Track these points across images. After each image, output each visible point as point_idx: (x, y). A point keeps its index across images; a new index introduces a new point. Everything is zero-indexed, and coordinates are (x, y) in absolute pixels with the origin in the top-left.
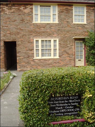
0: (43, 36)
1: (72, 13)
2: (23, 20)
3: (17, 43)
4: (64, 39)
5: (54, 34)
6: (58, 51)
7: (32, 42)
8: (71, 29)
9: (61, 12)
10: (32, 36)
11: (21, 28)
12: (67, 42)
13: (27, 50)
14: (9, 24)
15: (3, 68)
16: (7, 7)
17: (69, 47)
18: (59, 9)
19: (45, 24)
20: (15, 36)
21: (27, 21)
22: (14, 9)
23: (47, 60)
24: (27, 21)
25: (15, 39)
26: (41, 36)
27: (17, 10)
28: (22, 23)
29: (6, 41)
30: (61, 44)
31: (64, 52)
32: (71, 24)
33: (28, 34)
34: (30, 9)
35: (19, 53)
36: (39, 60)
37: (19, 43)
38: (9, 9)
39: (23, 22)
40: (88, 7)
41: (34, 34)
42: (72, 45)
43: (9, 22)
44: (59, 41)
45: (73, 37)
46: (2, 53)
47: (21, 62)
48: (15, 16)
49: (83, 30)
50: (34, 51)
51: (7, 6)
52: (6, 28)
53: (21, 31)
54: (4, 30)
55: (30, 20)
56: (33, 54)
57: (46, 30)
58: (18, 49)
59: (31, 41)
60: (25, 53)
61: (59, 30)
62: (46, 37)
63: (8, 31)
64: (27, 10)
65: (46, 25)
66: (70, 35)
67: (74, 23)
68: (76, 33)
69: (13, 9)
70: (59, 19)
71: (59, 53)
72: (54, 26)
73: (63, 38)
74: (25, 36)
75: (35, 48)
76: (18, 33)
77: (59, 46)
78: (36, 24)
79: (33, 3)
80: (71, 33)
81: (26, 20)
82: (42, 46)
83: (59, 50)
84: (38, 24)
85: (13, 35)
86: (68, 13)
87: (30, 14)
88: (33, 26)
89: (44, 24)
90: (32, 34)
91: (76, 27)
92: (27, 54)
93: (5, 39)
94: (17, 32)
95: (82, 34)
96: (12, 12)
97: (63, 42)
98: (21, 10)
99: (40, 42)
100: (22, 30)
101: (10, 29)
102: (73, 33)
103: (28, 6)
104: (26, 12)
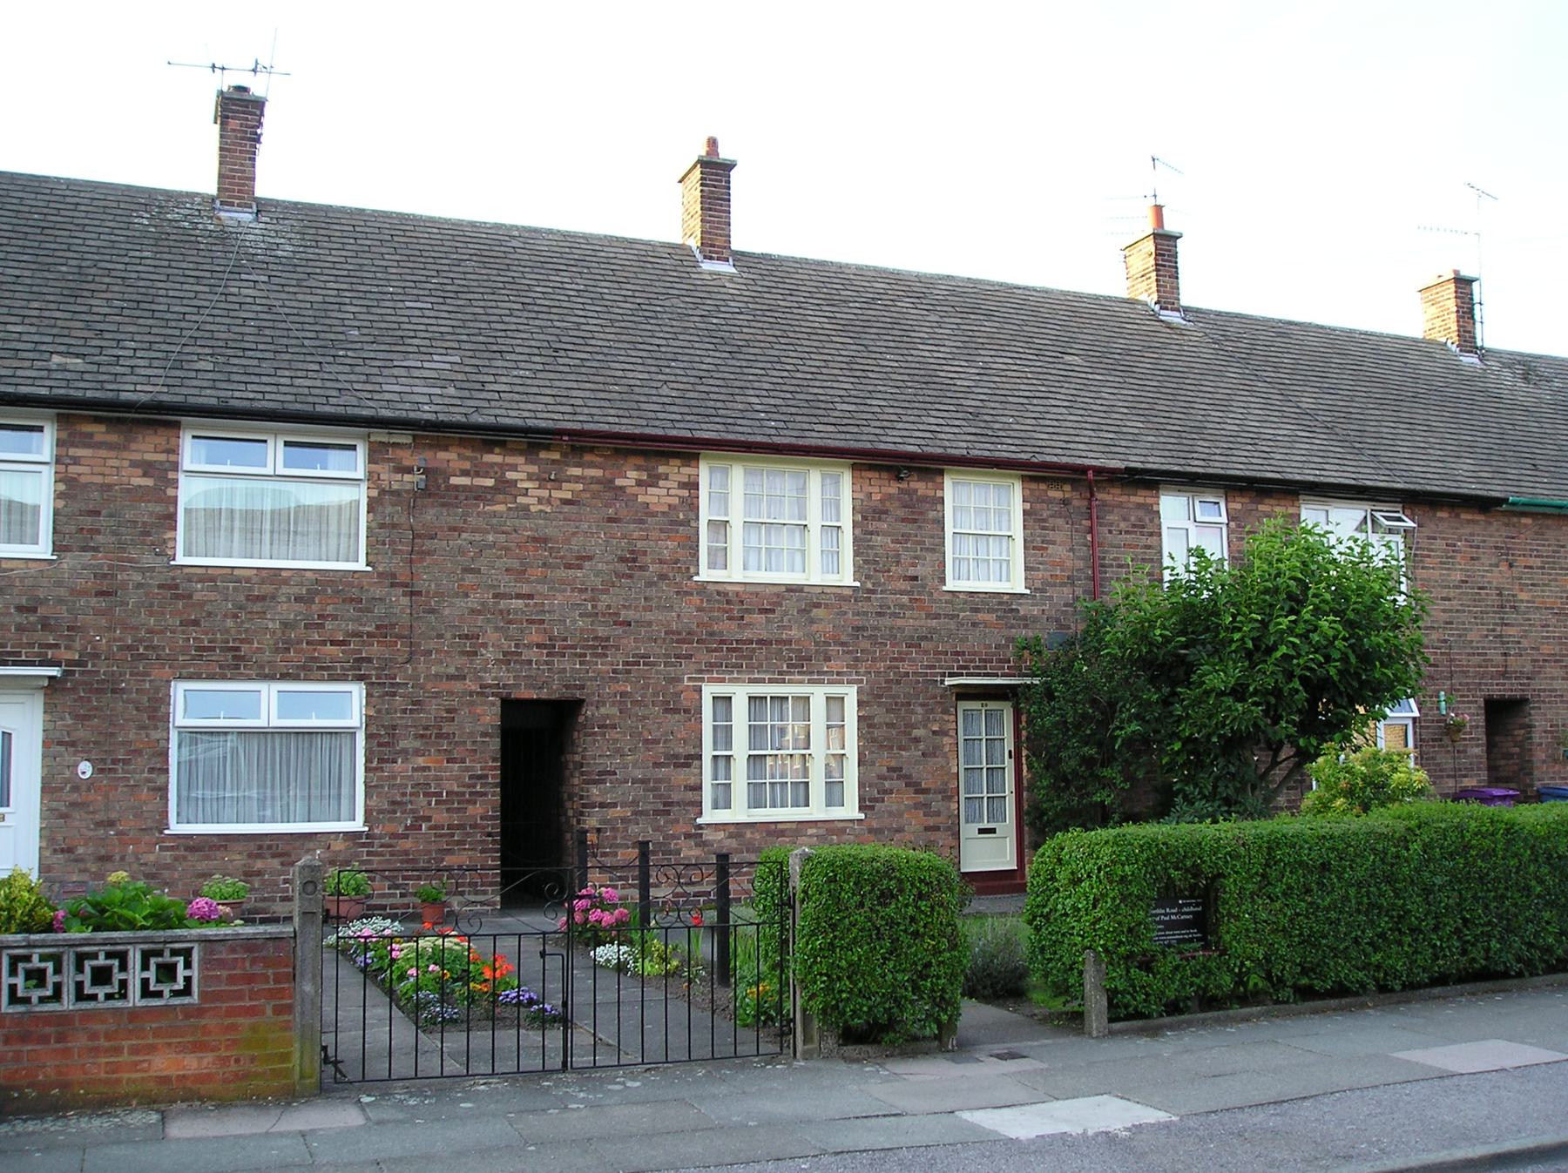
1: (941, 523)
2: (635, 560)
7: (686, 711)
10: (693, 667)
12: (913, 712)
13: (657, 765)
14: (543, 580)
15: (491, 884)
16: (534, 469)
17: (922, 747)
18: (861, 496)
22: (577, 479)
23: (782, 833)
28: (630, 576)
33: (668, 656)
34: (682, 485)
35: (603, 782)
36: (732, 829)
37: (602, 710)
38: (543, 481)
39: (638, 573)
40: (1033, 486)
41: (704, 657)
44: (860, 704)
45: (949, 681)
47: (618, 846)
49: (1005, 632)
53: (620, 630)
54: (510, 622)
56: (699, 788)
60: (643, 781)
61: (857, 629)
62: (780, 673)
63: (534, 627)
65: (778, 595)
67: (951, 585)
71: (861, 785)
72: (827, 606)
73: (887, 682)
75: (708, 752)
76: (602, 646)
78: (720, 588)
80: (937, 653)
82: (755, 732)
86: (915, 521)
88: (696, 599)
95: (1000, 661)
96: (566, 502)
98: (622, 488)
99: (740, 708)
101: (547, 617)
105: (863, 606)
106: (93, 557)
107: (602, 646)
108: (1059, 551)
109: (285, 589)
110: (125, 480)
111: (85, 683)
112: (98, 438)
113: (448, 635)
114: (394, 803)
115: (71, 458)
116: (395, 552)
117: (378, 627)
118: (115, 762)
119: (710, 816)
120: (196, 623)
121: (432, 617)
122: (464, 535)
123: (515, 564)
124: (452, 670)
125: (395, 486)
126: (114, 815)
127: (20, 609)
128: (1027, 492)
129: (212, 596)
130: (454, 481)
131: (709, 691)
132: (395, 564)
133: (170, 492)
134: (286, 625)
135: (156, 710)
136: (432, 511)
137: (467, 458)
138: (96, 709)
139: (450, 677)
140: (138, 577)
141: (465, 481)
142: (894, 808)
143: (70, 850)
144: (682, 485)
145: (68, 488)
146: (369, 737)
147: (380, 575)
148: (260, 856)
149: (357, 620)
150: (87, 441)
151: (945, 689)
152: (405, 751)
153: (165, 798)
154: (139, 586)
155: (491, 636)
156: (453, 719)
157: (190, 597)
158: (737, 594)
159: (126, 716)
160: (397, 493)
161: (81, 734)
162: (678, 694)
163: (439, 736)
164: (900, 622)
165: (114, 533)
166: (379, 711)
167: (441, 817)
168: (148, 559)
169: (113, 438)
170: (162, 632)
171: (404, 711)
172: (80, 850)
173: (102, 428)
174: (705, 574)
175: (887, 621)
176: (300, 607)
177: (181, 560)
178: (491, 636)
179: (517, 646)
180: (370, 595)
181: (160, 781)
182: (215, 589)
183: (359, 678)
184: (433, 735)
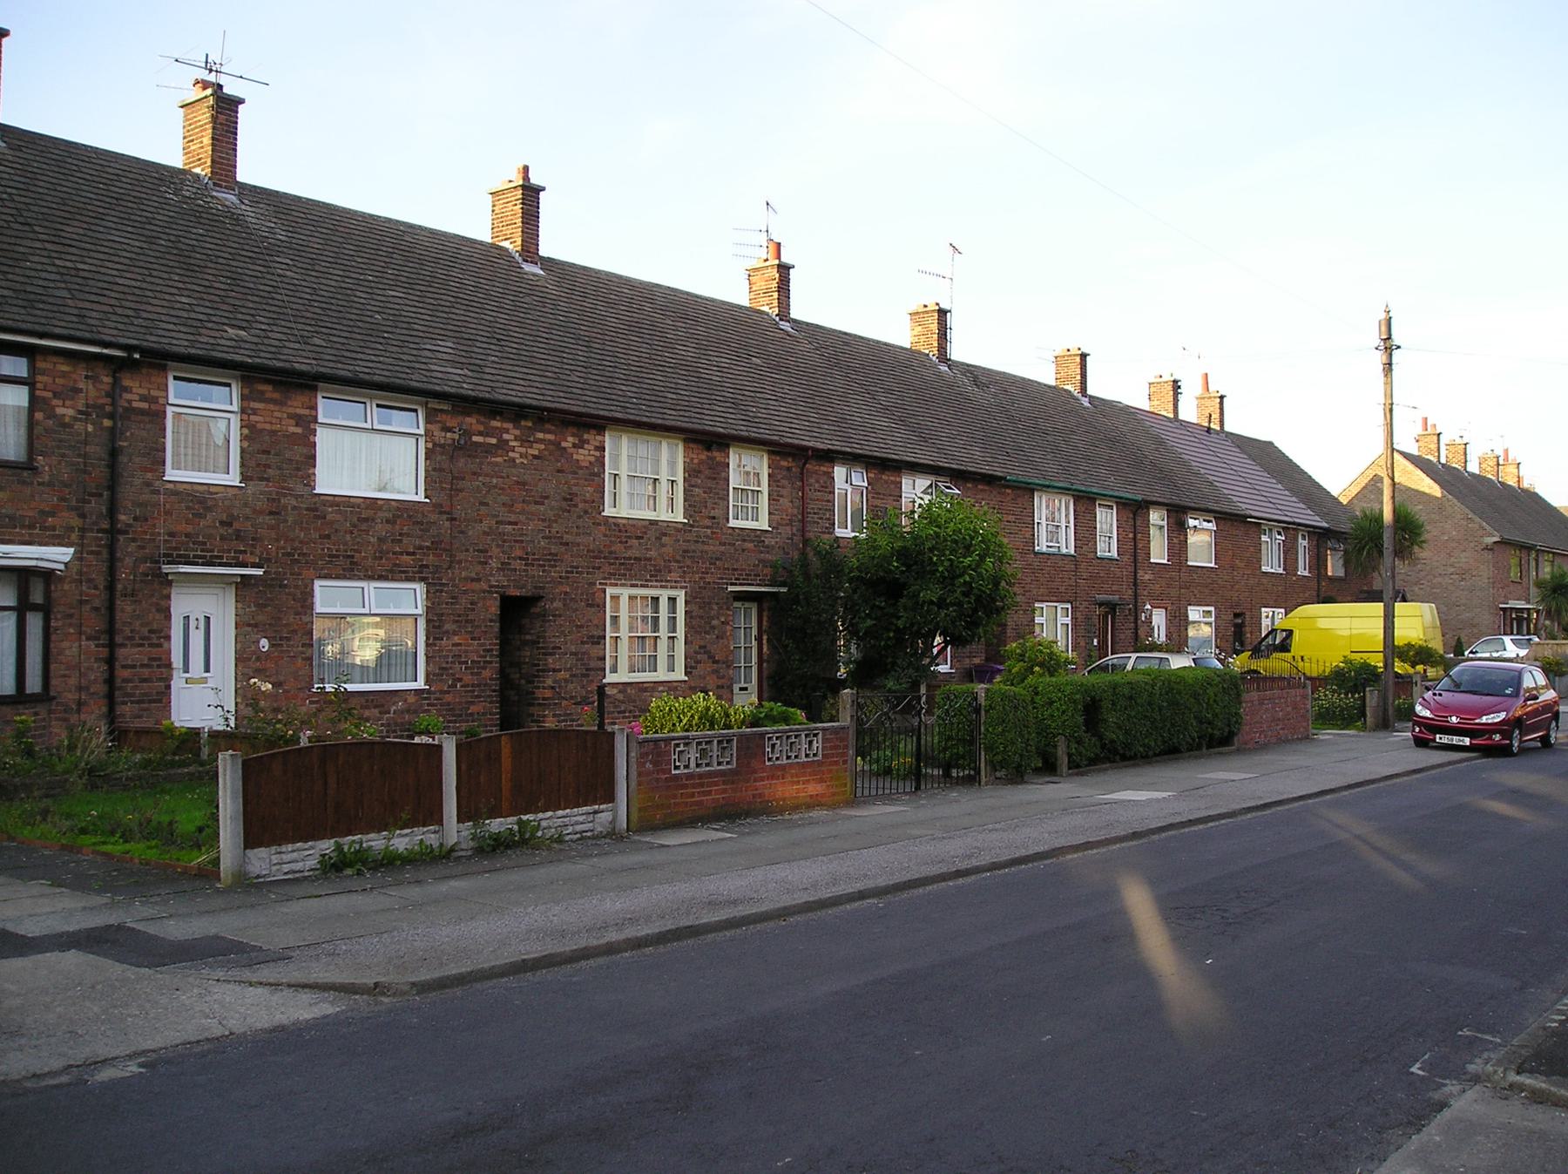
16: (517, 432)
23: (646, 690)
41: (607, 569)
45: (731, 588)
60: (575, 654)
67: (733, 523)
75: (608, 634)
76: (554, 559)
96: (535, 457)
99: (624, 602)
107: (554, 559)
108: (785, 502)
109: (380, 514)
112: (268, 395)
116: (443, 489)
120: (328, 537)
127: (222, 523)
129: (338, 517)
130: (475, 439)
139: (473, 580)
140: (294, 502)
145: (251, 433)
146: (428, 621)
147: (434, 505)
148: (367, 707)
152: (447, 632)
154: (294, 508)
155: (495, 551)
161: (260, 618)
167: (468, 679)
169: (276, 395)
173: (270, 388)
174: (609, 511)
176: (389, 527)
178: (495, 551)
183: (422, 579)
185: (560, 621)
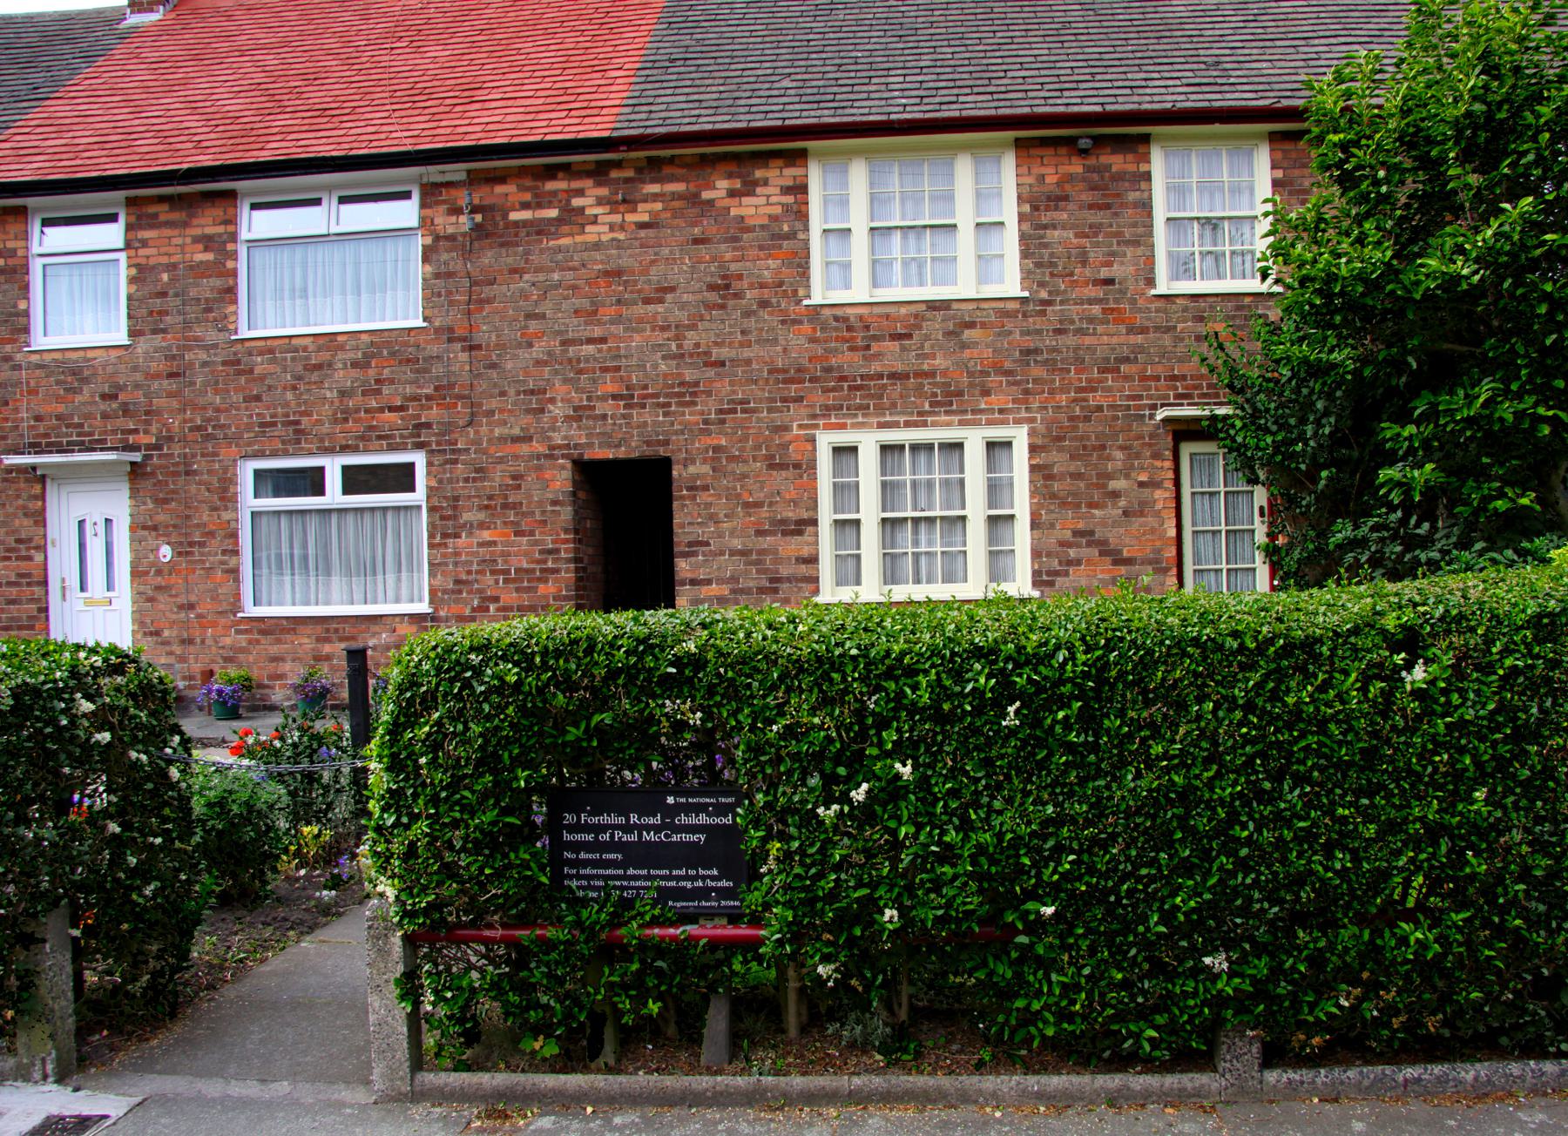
0: (894, 405)
1: (1146, 207)
2: (727, 287)
3: (675, 473)
4: (1075, 428)
5: (986, 393)
6: (1022, 537)
7: (797, 466)
8: (1139, 339)
9: (1049, 199)
10: (804, 412)
11: (714, 351)
12: (1109, 458)
13: (760, 533)
14: (618, 320)
16: (604, 192)
17: (1122, 503)
19: (913, 309)
20: (666, 414)
21: (762, 286)
22: (655, 197)
24: (762, 286)
25: (659, 443)
26: (880, 409)
27: (676, 204)
28: (723, 307)
29: (588, 455)
30: (1049, 477)
31: (1079, 546)
32: (1141, 303)
34: (787, 190)
35: (694, 554)
37: (692, 469)
38: (613, 204)
39: (731, 303)
40: (1288, 146)
41: (818, 399)
42: (1154, 484)
43: (619, 302)
44: (1033, 449)
45: (1161, 415)
46: (557, 551)
48: (666, 251)
50: (816, 535)
51: (599, 184)
52: (591, 348)
53: (711, 373)
54: (580, 372)
55: (781, 284)
56: (813, 560)
57: (926, 356)
58: (686, 520)
59: (794, 453)
60: (743, 553)
61: (1027, 352)
62: (920, 414)
63: (608, 376)
64: (763, 200)
65: (916, 316)
66: (1130, 398)
68: (1184, 378)
69: (646, 201)
70: (1029, 263)
71: (1036, 554)
72: (983, 325)
73: (1071, 419)
74: (744, 411)
75: (826, 514)
76: (689, 393)
77: (1033, 494)
78: (839, 312)
79: (810, 145)
80: (1144, 378)
81: (751, 286)
82: (889, 491)
83: (1035, 524)
84: (849, 311)
85: (643, 406)
86: (1108, 207)
87: (787, 236)
88: (806, 327)
89: (903, 311)
90: (799, 399)
91: (1180, 326)
92: (758, 562)
93: (584, 441)
94: (682, 384)
96: (642, 226)
97: (1072, 458)
98: (711, 203)
100: (723, 364)
102: (1158, 379)
103: (766, 166)
104: (752, 222)
105: (1034, 322)
106: (164, 339)
109: (340, 356)
110: (188, 257)
111: (161, 467)
112: (162, 218)
113: (512, 392)
114: (457, 582)
115: (140, 241)
116: (451, 304)
117: (437, 388)
118: (191, 544)
119: (830, 593)
120: (258, 398)
121: (494, 374)
122: (526, 277)
123: (585, 303)
124: (516, 431)
125: (450, 230)
126: (193, 598)
127: (104, 397)
128: (1279, 155)
129: (272, 368)
130: (514, 216)
131: (826, 441)
132: (454, 317)
133: (230, 264)
134: (343, 394)
135: (226, 490)
136: (489, 254)
137: (527, 189)
138: (174, 492)
139: (516, 440)
140: (203, 356)
141: (526, 215)
142: (1084, 582)
143: (157, 633)
144: (787, 190)
146: (431, 509)
147: (437, 331)
148: (328, 640)
149: (415, 382)
150: (153, 222)
151: (1157, 427)
153: (237, 580)
154: (205, 364)
155: (559, 389)
156: (519, 487)
157: (251, 371)
158: (861, 318)
159: (200, 498)
160: (451, 238)
161: (162, 518)
162: (784, 446)
163: (505, 506)
164: (1088, 340)
165: (179, 313)
166: (440, 481)
168: (212, 336)
169: (176, 216)
170: (227, 410)
171: (466, 480)
172: (166, 633)
173: (166, 207)
175: (1070, 340)
176: (355, 373)
177: (244, 333)
178: (559, 389)
179: (589, 399)
180: (427, 353)
181: (233, 561)
182: (274, 361)
183: (419, 446)
184: (499, 505)
185: (702, 497)
